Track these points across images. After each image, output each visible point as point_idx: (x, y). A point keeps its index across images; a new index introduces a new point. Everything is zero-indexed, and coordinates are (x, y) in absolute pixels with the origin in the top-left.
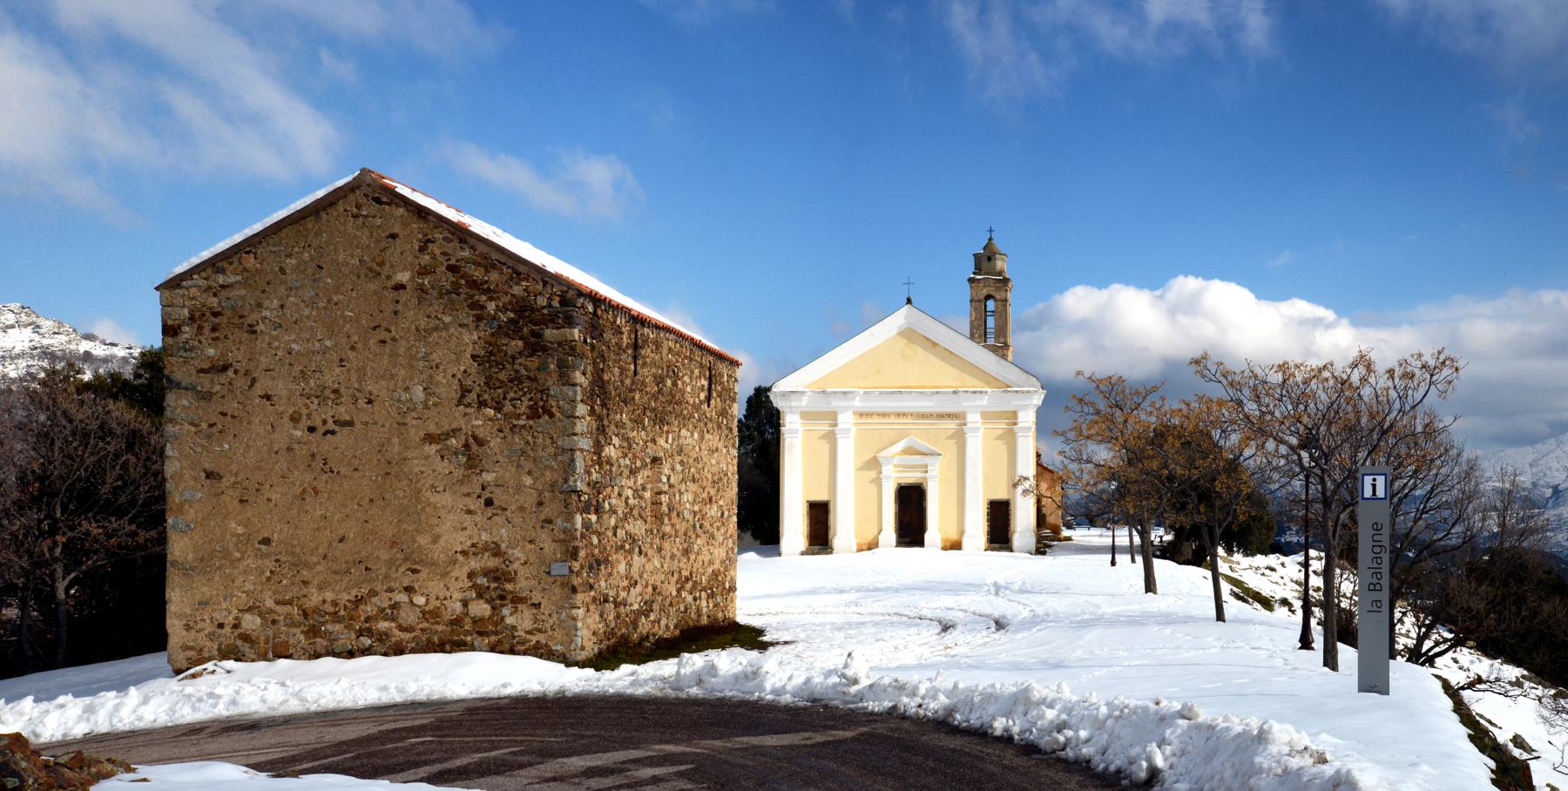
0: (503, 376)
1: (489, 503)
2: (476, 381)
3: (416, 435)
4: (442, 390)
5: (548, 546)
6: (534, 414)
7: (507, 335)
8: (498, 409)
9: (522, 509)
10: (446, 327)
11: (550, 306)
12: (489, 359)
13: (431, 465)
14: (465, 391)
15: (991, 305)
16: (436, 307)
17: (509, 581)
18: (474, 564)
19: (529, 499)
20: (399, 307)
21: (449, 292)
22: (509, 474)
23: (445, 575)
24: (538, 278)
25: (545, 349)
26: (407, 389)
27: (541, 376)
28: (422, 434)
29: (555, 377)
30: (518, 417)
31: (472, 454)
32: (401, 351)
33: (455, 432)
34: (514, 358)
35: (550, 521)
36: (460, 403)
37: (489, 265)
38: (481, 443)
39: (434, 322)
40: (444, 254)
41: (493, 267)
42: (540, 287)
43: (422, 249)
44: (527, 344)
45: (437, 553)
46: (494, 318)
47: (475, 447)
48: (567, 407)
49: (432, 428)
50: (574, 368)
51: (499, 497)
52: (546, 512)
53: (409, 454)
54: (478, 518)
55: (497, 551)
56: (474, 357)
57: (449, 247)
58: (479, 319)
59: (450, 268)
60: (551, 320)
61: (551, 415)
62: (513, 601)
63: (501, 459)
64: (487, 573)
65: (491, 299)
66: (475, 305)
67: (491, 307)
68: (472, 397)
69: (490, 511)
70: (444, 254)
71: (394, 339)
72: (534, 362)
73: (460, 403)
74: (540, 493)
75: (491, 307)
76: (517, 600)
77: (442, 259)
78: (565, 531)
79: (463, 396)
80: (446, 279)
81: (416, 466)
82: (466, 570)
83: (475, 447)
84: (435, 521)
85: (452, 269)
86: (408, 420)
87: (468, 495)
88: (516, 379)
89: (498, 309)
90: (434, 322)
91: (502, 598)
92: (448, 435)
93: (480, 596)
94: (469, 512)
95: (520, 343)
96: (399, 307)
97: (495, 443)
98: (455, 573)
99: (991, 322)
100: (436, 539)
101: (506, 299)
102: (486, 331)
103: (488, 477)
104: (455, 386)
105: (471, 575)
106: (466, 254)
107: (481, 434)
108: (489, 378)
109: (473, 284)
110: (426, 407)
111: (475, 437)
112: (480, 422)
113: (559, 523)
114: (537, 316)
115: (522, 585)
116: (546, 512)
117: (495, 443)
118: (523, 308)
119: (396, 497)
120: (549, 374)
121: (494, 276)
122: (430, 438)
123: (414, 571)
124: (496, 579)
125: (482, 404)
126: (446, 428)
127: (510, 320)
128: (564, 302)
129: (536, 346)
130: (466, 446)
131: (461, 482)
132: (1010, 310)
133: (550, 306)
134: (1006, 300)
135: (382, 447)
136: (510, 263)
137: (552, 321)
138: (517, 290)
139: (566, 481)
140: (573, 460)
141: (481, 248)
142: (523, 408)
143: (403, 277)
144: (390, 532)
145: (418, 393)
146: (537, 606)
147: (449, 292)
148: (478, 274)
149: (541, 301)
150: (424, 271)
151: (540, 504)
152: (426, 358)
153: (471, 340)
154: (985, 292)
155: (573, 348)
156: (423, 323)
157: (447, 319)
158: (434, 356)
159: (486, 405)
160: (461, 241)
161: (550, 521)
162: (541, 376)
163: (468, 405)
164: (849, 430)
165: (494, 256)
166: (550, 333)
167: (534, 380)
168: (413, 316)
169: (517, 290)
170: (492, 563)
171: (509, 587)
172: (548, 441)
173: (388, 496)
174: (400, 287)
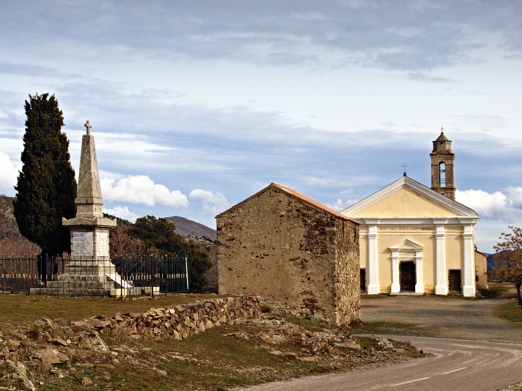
0: (312, 242)
1: (309, 279)
2: (304, 243)
3: (287, 258)
4: (294, 246)
5: (327, 293)
6: (322, 253)
7: (314, 229)
8: (311, 251)
9: (319, 281)
10: (296, 227)
11: (327, 221)
12: (309, 236)
13: (292, 268)
14: (301, 246)
15: (443, 167)
16: (293, 222)
17: (315, 302)
18: (305, 297)
19: (321, 278)
20: (282, 222)
21: (296, 217)
22: (315, 271)
23: (296, 300)
24: (323, 212)
25: (325, 234)
26: (284, 245)
27: (324, 242)
28: (289, 258)
29: (329, 242)
30: (318, 254)
31: (303, 264)
32: (282, 235)
33: (298, 258)
34: (316, 236)
35: (328, 285)
36: (300, 249)
37: (309, 209)
38: (306, 261)
39: (292, 226)
40: (295, 206)
41: (310, 210)
42: (324, 215)
43: (288, 205)
44: (320, 232)
45: (294, 293)
46: (310, 225)
47: (304, 262)
48: (332, 251)
49: (292, 257)
50: (334, 239)
51: (312, 277)
52: (326, 282)
53: (285, 264)
54: (306, 283)
55: (311, 294)
56: (304, 236)
57: (296, 204)
58: (305, 225)
59: (297, 210)
60: (328, 225)
61: (328, 253)
62: (317, 309)
63: (312, 266)
64: (308, 300)
65: (309, 219)
66: (304, 221)
67: (309, 221)
68: (303, 248)
69: (309, 282)
70: (295, 206)
71: (280, 231)
72: (322, 237)
73: (300, 249)
74: (325, 276)
75: (309, 221)
76: (318, 308)
77: (294, 207)
78: (332, 288)
79: (301, 247)
80: (295, 213)
81: (288, 268)
82: (302, 299)
83: (304, 262)
84: (293, 284)
85: (297, 210)
86: (285, 254)
87: (303, 277)
88: (317, 242)
89: (311, 222)
90: (292, 226)
91: (313, 307)
92: (296, 259)
93: (306, 307)
94: (303, 282)
95: (318, 232)
96: (282, 222)
97: (311, 261)
98: (299, 300)
99: (443, 176)
100: (293, 289)
101: (313, 219)
102: (307, 229)
103: (309, 271)
104: (298, 244)
105: (304, 300)
106: (301, 206)
107: (306, 258)
108: (308, 242)
109: (304, 215)
110: (290, 251)
111: (304, 260)
112: (307, 255)
113: (331, 285)
114: (323, 224)
115: (319, 304)
116: (326, 282)
117: (311, 261)
118: (319, 222)
119: (281, 277)
120: (327, 241)
121: (310, 212)
122: (291, 260)
123: (287, 298)
124: (311, 302)
125: (306, 250)
126: (296, 257)
127: (315, 225)
128: (331, 219)
129: (323, 233)
130: (302, 262)
131: (301, 273)
132: (454, 169)
133: (327, 221)
134: (452, 165)
135: (277, 262)
136: (315, 208)
137: (328, 225)
138: (317, 216)
139: (333, 273)
140: (335, 267)
141: (306, 204)
142: (319, 251)
143: (283, 213)
144: (280, 287)
145: (288, 246)
146: (324, 310)
147: (296, 217)
148: (305, 212)
149: (325, 219)
150: (289, 211)
151: (325, 280)
152: (290, 236)
153: (303, 231)
154: (440, 161)
155: (334, 233)
156: (289, 227)
157: (296, 225)
158: (292, 236)
159: (308, 250)
160: (300, 202)
161: (328, 285)
162: (324, 242)
163: (302, 250)
164: (375, 236)
165: (310, 206)
166: (327, 229)
167: (322, 243)
168: (286, 224)
169: (317, 216)
170: (310, 297)
171: (315, 304)
172: (327, 261)
173: (279, 276)
174: (282, 216)
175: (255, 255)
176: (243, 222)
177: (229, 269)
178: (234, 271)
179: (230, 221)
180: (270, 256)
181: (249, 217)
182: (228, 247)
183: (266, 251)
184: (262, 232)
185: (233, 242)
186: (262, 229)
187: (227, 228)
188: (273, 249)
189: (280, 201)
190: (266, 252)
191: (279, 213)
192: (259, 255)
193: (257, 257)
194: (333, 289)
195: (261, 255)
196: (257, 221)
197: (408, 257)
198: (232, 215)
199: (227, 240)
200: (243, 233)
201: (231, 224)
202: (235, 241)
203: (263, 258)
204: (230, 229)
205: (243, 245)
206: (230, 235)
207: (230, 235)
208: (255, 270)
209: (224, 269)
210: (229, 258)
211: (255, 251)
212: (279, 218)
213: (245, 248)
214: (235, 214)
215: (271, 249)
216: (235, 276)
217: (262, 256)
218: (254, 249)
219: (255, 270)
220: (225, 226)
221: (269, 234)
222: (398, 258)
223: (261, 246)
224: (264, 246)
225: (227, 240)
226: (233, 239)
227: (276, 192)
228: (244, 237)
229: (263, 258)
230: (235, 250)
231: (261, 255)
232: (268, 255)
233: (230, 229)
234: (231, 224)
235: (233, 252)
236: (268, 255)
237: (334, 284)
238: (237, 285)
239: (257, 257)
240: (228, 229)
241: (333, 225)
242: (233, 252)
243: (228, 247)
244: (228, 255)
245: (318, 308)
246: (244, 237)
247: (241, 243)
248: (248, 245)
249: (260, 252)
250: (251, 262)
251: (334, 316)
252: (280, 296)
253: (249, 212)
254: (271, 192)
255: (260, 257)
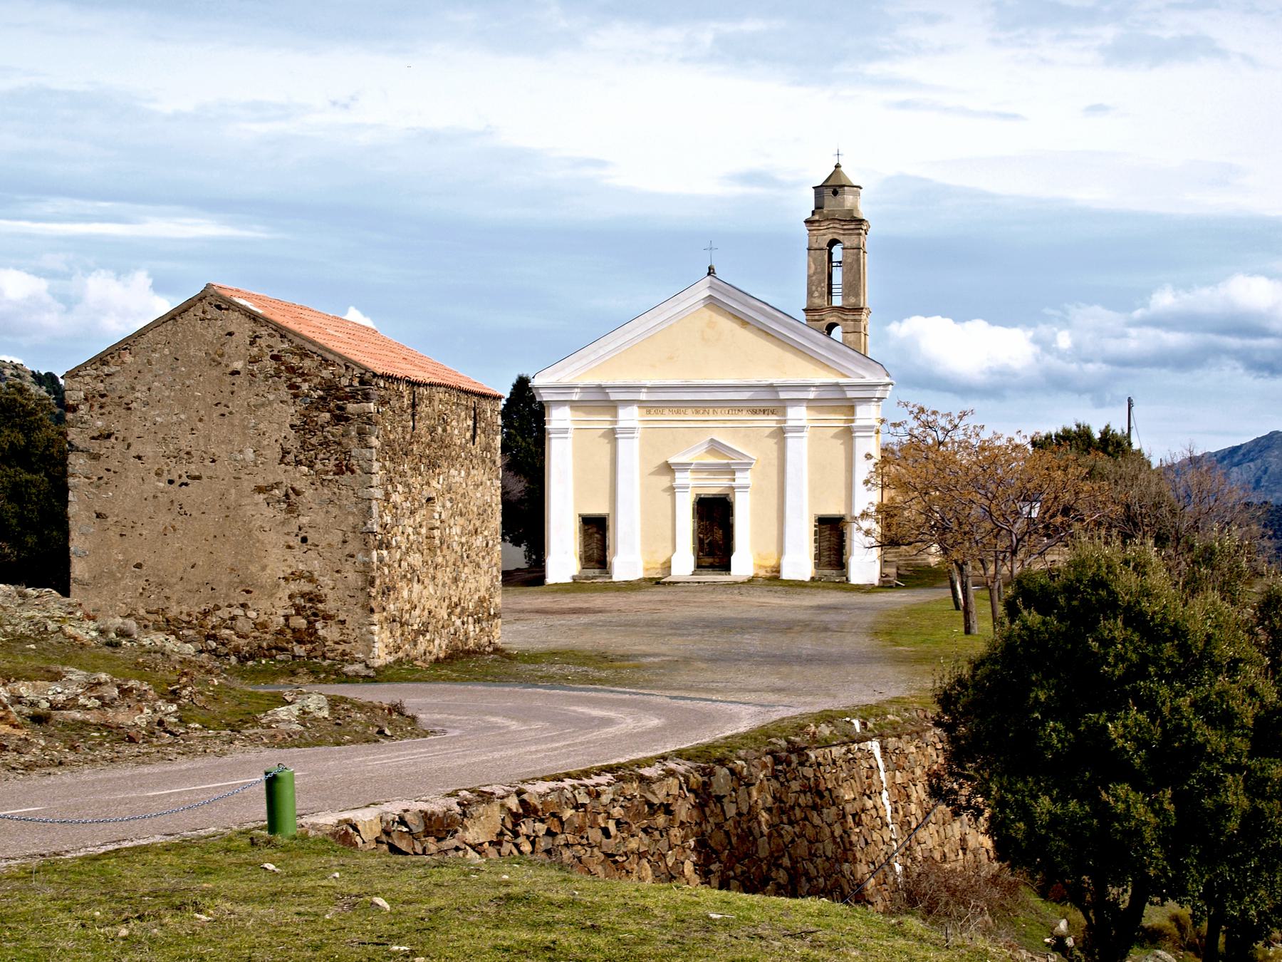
0: (314, 441)
1: (304, 540)
2: (293, 443)
3: (248, 484)
4: (267, 452)
6: (339, 472)
7: (317, 408)
8: (311, 467)
9: (330, 545)
10: (271, 403)
11: (351, 385)
12: (305, 427)
13: (262, 512)
14: (285, 452)
16: (263, 388)
17: (321, 602)
18: (294, 587)
19: (336, 537)
20: (235, 388)
21: (272, 376)
22: (319, 518)
23: (271, 596)
25: (347, 419)
26: (241, 452)
27: (345, 441)
29: (356, 441)
30: (327, 473)
32: (236, 422)
33: (277, 485)
34: (323, 427)
36: (281, 461)
37: (304, 355)
38: (297, 493)
40: (269, 346)
41: (307, 355)
42: (343, 371)
43: (252, 343)
45: (266, 578)
47: (293, 496)
48: (365, 465)
49: (261, 483)
50: (371, 434)
51: (312, 536)
54: (296, 552)
56: (292, 426)
57: (272, 341)
58: (295, 396)
59: (273, 357)
60: (352, 397)
61: (353, 472)
62: (324, 618)
64: (303, 595)
65: (305, 381)
67: (305, 387)
68: (290, 457)
69: (305, 547)
70: (269, 346)
71: (231, 413)
72: (339, 430)
73: (281, 461)
75: (305, 387)
76: (327, 617)
77: (266, 350)
78: (364, 564)
79: (284, 457)
80: (269, 365)
81: (249, 510)
82: (288, 592)
83: (293, 496)
84: (263, 554)
85: (275, 358)
86: (242, 476)
87: (288, 534)
88: (325, 443)
89: (310, 389)
91: (315, 615)
92: (272, 488)
93: (298, 614)
94: (289, 547)
95: (328, 415)
96: (235, 388)
97: (309, 493)
98: (280, 594)
100: (264, 568)
101: (316, 381)
103: (304, 520)
104: (278, 449)
105: (291, 597)
106: (285, 346)
107: (297, 486)
108: (304, 442)
109: (291, 370)
111: (293, 489)
112: (299, 477)
113: (360, 557)
115: (330, 606)
116: (349, 549)
118: (330, 388)
119: (234, 535)
121: (307, 363)
122: (260, 490)
123: (248, 592)
124: (310, 600)
125: (299, 463)
126: (271, 481)
127: (320, 398)
128: (362, 382)
129: (340, 418)
130: (287, 495)
131: (283, 523)
133: (351, 385)
136: (320, 352)
137: (353, 397)
138: (326, 374)
139: (365, 524)
140: (370, 508)
141: (297, 341)
142: (331, 465)
143: (238, 365)
144: (229, 561)
145: (250, 455)
146: (343, 622)
148: (295, 361)
149: (345, 382)
150: (254, 360)
151: (345, 542)
153: (291, 412)
154: (830, 237)
156: (253, 401)
157: (271, 397)
158: (261, 426)
160: (282, 336)
161: (352, 556)
165: (308, 346)
166: (351, 407)
167: (339, 444)
168: (245, 396)
169: (326, 374)
170: (307, 587)
171: (320, 605)
173: (227, 534)
175: (166, 477)
176: (133, 388)
177: (99, 516)
178: (111, 520)
179: (101, 386)
180: (205, 479)
181: (149, 377)
182: (96, 457)
183: (193, 466)
184: (183, 417)
185: (108, 443)
186: (185, 408)
187: (91, 406)
188: (213, 461)
189: (230, 334)
190: (194, 469)
191: (227, 366)
192: (175, 477)
193: (171, 482)
194: (367, 565)
195: (180, 477)
196: (171, 388)
197: (714, 486)
198: (106, 369)
199: (93, 438)
200: (134, 418)
201: (103, 396)
202: (113, 440)
203: (186, 484)
204: (101, 407)
205: (133, 452)
206: (99, 423)
207: (99, 423)
208: (165, 519)
209: (84, 514)
210: (98, 487)
211: (166, 468)
212: (229, 379)
213: (139, 458)
214: (113, 369)
215: (207, 462)
216: (113, 534)
217: (185, 479)
218: (163, 461)
219: (165, 519)
220: (86, 399)
221: (201, 420)
222: (691, 487)
223: (182, 454)
224: (188, 453)
225: (93, 438)
226: (109, 436)
227: (219, 307)
228: (137, 430)
229: (186, 484)
230: (114, 464)
231: (180, 477)
232: (199, 478)
233: (101, 407)
234: (103, 396)
235: (108, 470)
236: (199, 478)
237: (368, 552)
238: (120, 557)
239: (171, 482)
240: (96, 407)
241: (367, 398)
242: (108, 470)
243: (96, 457)
244: (95, 478)
245: (327, 617)
246: (137, 430)
247: (129, 445)
248: (148, 450)
249: (178, 470)
250: (155, 497)
251: (370, 636)
252: (230, 584)
253: (149, 363)
254: (208, 308)
255: (178, 482)
